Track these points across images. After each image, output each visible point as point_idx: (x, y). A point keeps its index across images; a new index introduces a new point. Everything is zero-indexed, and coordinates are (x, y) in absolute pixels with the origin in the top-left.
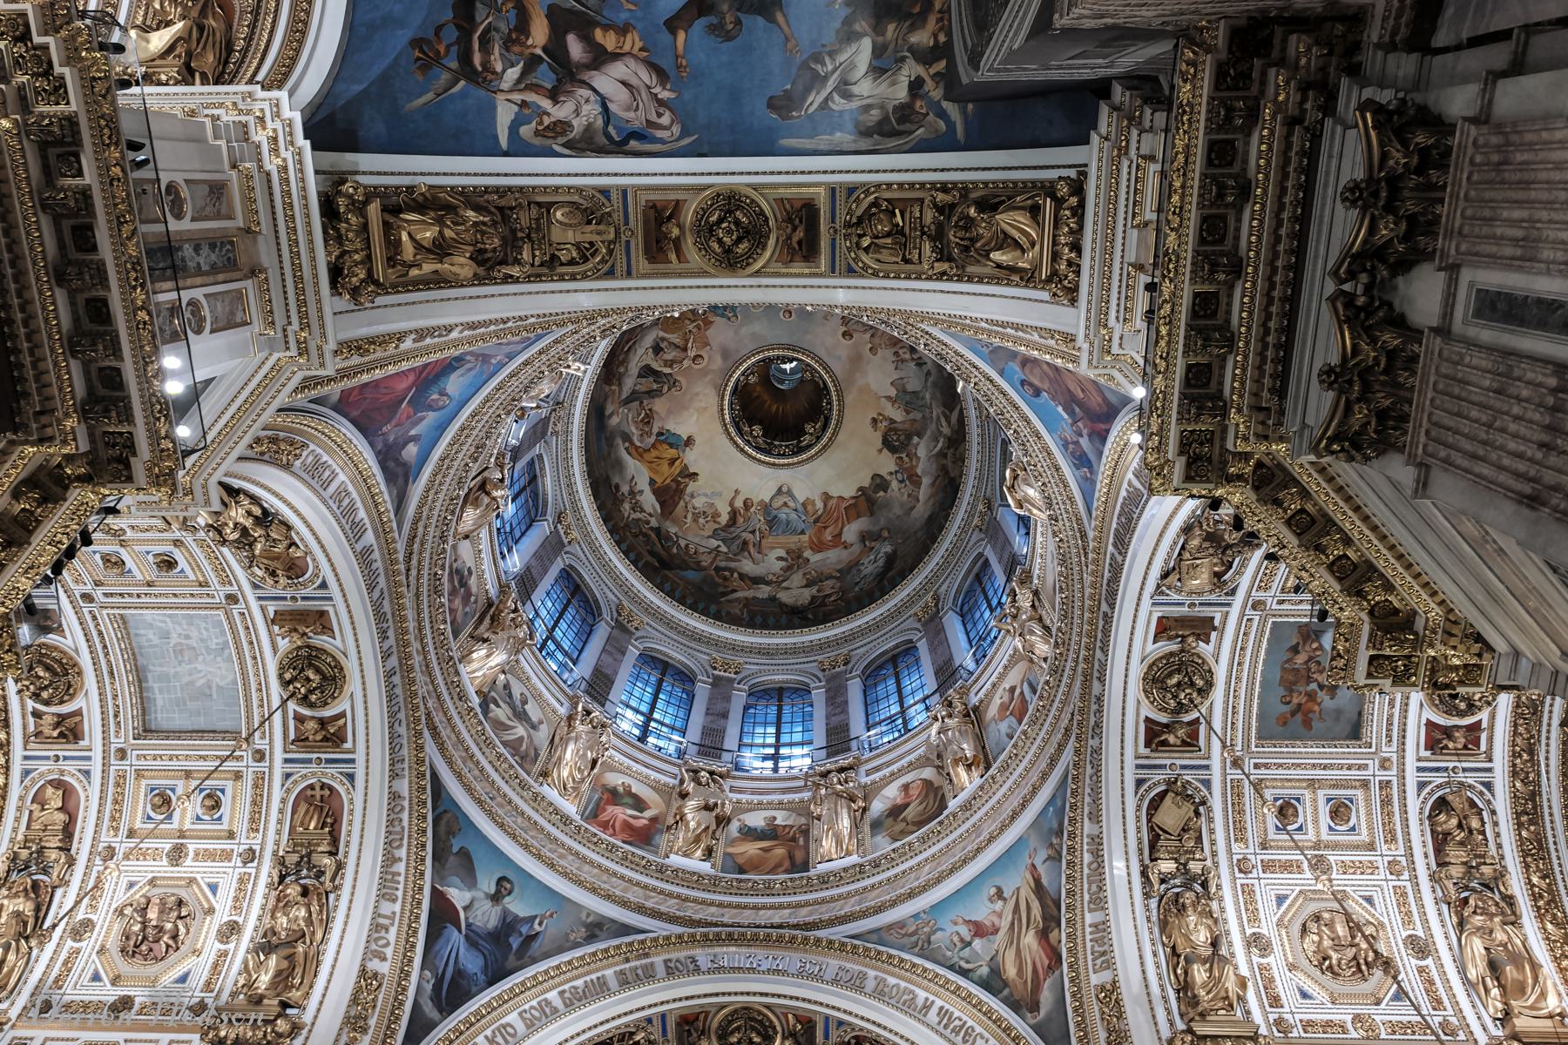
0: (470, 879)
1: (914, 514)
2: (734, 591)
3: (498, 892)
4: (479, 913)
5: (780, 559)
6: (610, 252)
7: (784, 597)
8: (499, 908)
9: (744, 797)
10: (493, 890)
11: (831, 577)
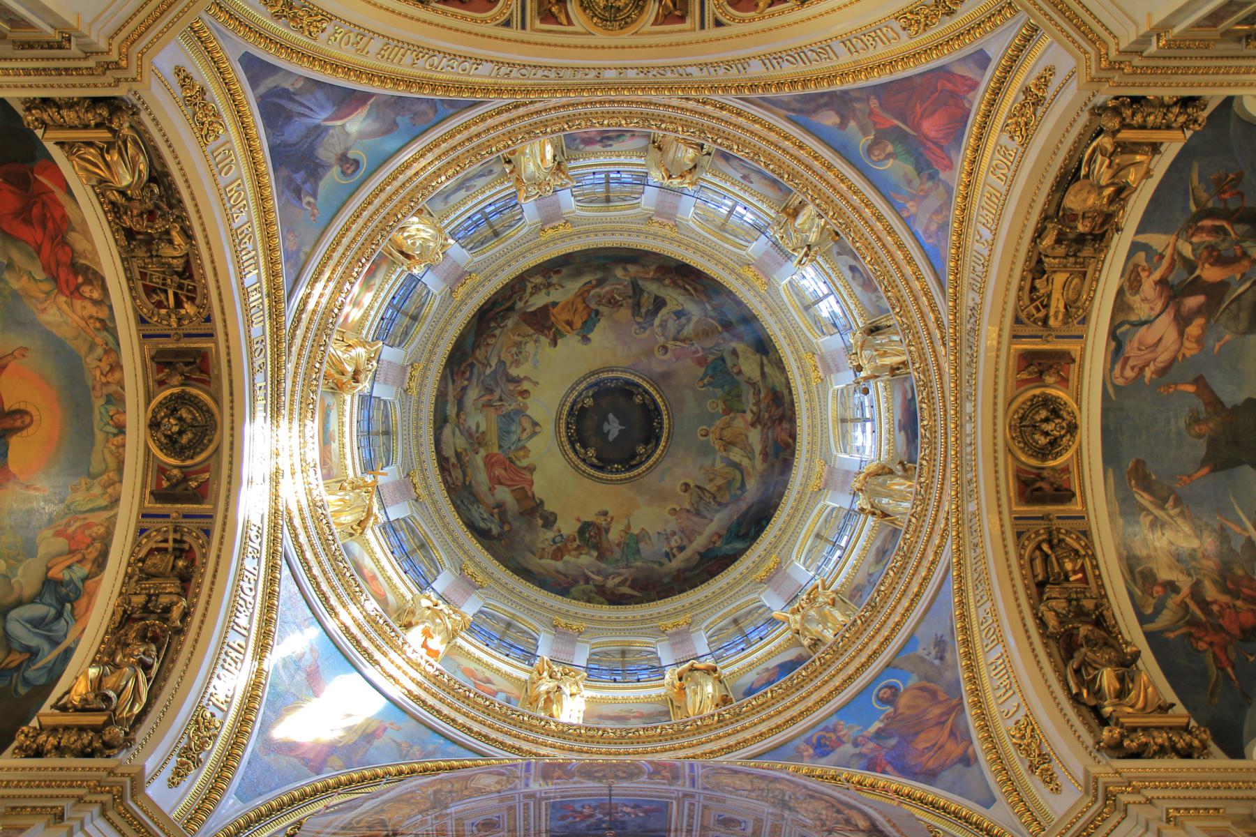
1: (529, 555)
5: (478, 427)
6: (1035, 322)
7: (448, 430)
8: (333, 161)
9: (347, 407)
10: (351, 155)
11: (465, 475)
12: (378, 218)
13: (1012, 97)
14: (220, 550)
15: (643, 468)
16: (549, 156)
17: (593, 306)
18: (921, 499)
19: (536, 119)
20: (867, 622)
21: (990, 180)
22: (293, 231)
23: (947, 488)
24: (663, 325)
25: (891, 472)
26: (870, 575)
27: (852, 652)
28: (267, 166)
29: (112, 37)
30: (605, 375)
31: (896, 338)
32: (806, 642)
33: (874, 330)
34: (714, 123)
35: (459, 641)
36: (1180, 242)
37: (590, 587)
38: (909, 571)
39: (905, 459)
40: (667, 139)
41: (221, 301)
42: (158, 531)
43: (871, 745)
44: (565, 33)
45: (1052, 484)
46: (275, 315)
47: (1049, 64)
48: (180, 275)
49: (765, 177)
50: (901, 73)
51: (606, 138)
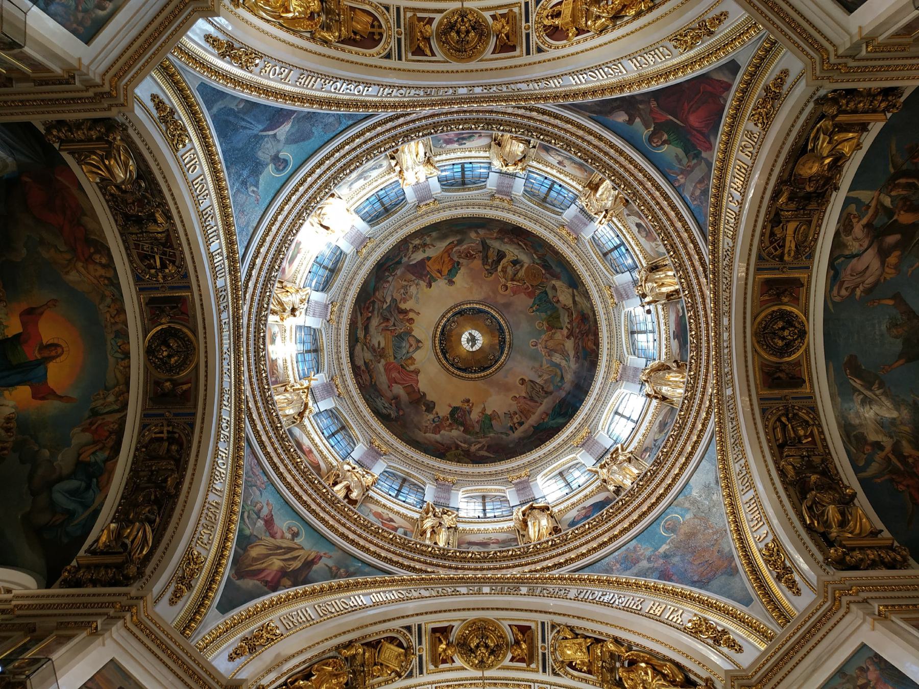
0: (295, 139)
1: (417, 431)
2: (361, 314)
3: (279, 159)
4: (269, 145)
5: (379, 343)
6: (773, 258)
7: (358, 347)
10: (281, 155)
12: (303, 201)
13: (758, 92)
14: (201, 437)
15: (493, 369)
16: (422, 154)
17: (456, 259)
18: (691, 388)
19: (412, 126)
20: (655, 473)
21: (739, 157)
22: (243, 212)
23: (710, 377)
24: (504, 270)
25: (668, 368)
26: (655, 441)
27: (644, 495)
28: (222, 166)
29: (104, 75)
30: (465, 306)
31: (671, 273)
32: (612, 488)
33: (654, 268)
34: (538, 124)
35: (371, 493)
36: (882, 196)
37: (459, 451)
38: (684, 437)
39: (678, 358)
40: (505, 138)
41: (194, 262)
42: (156, 426)
43: (661, 561)
44: (430, 61)
45: (787, 374)
46: (234, 271)
47: (784, 68)
48: (164, 245)
49: (575, 162)
50: (673, 81)
51: (461, 139)
